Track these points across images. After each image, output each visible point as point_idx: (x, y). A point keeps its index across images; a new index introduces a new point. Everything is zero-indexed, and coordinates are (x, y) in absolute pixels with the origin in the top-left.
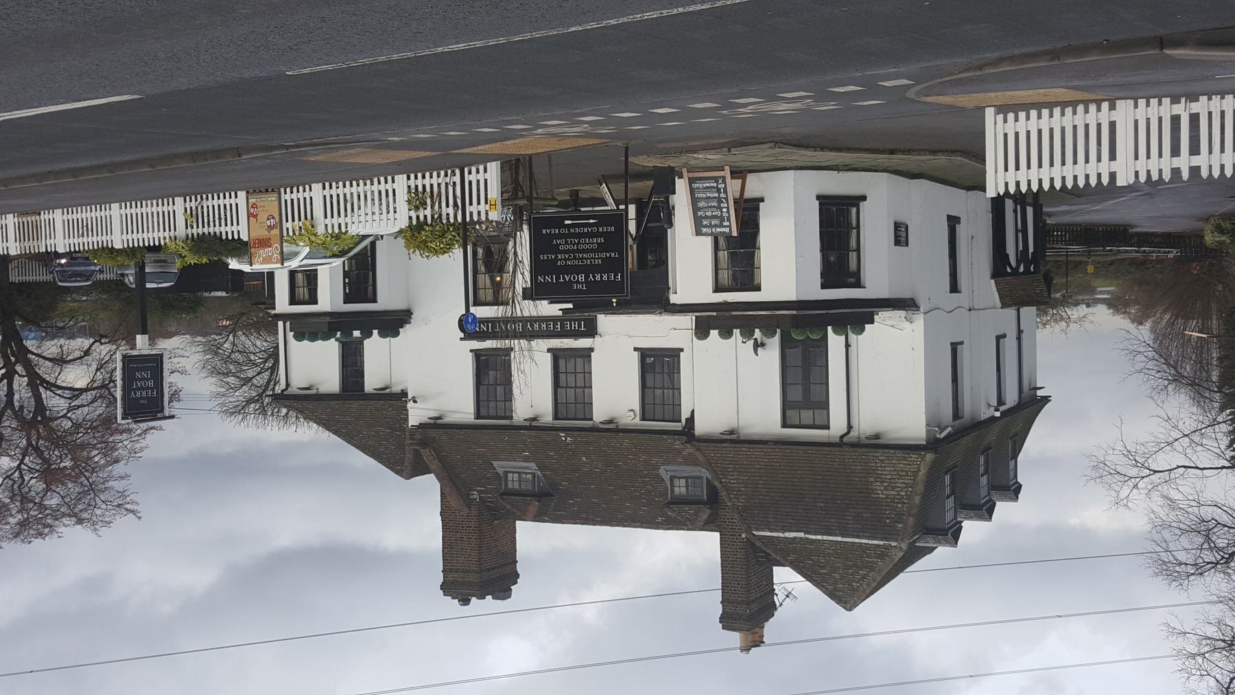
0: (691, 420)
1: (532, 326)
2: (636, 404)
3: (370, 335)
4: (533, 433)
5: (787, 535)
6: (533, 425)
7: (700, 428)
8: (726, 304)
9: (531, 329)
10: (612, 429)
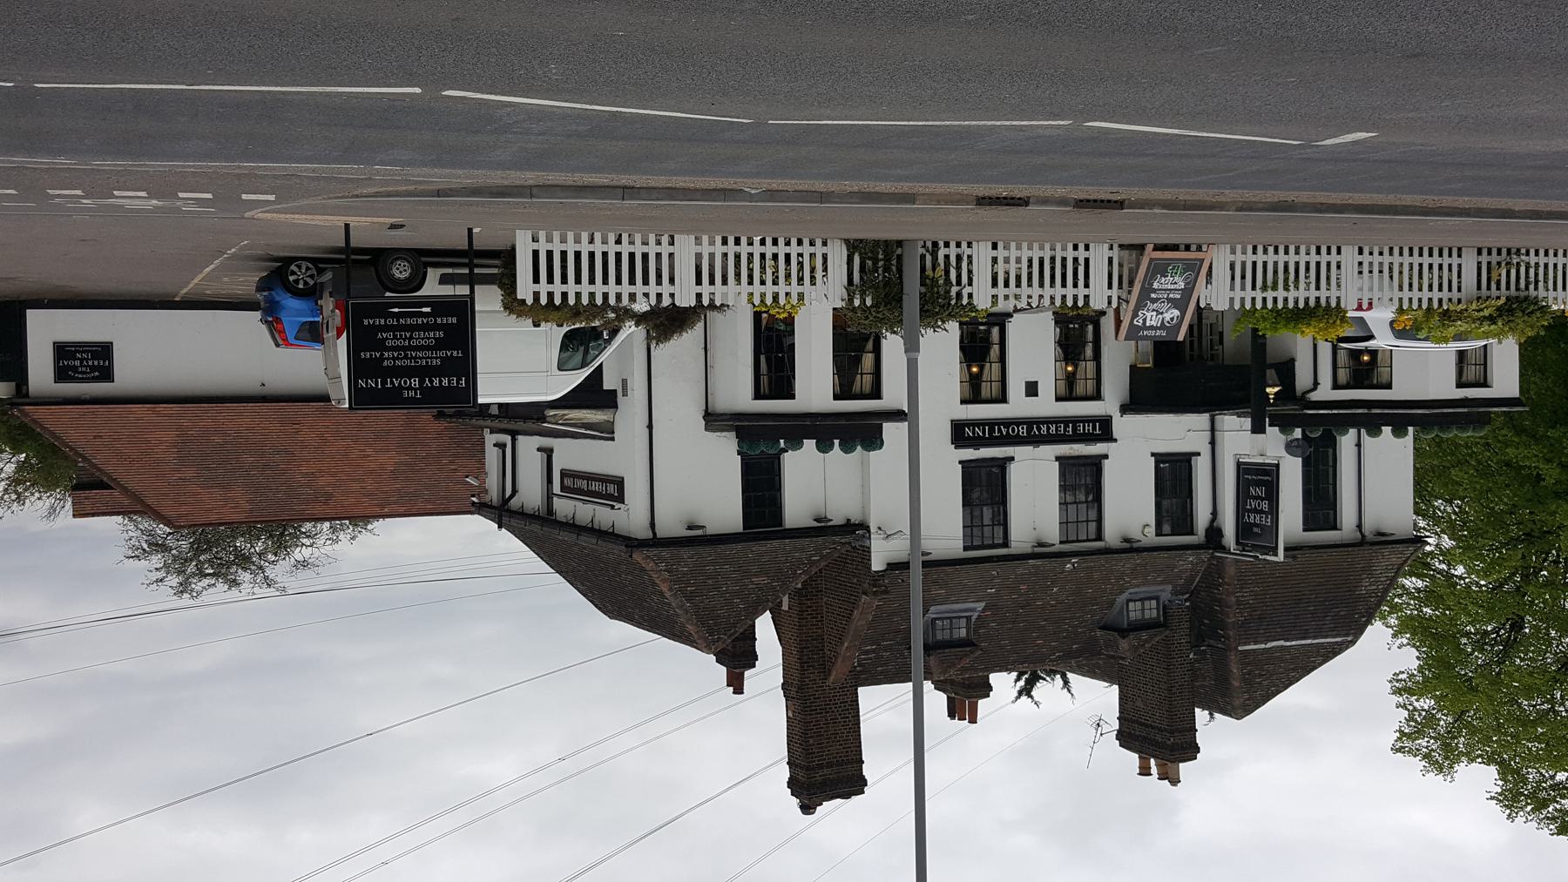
1: (1039, 429)
2: (1150, 516)
3: (798, 445)
6: (1040, 553)
8: (1466, 399)
9: (1034, 432)
10: (1130, 547)
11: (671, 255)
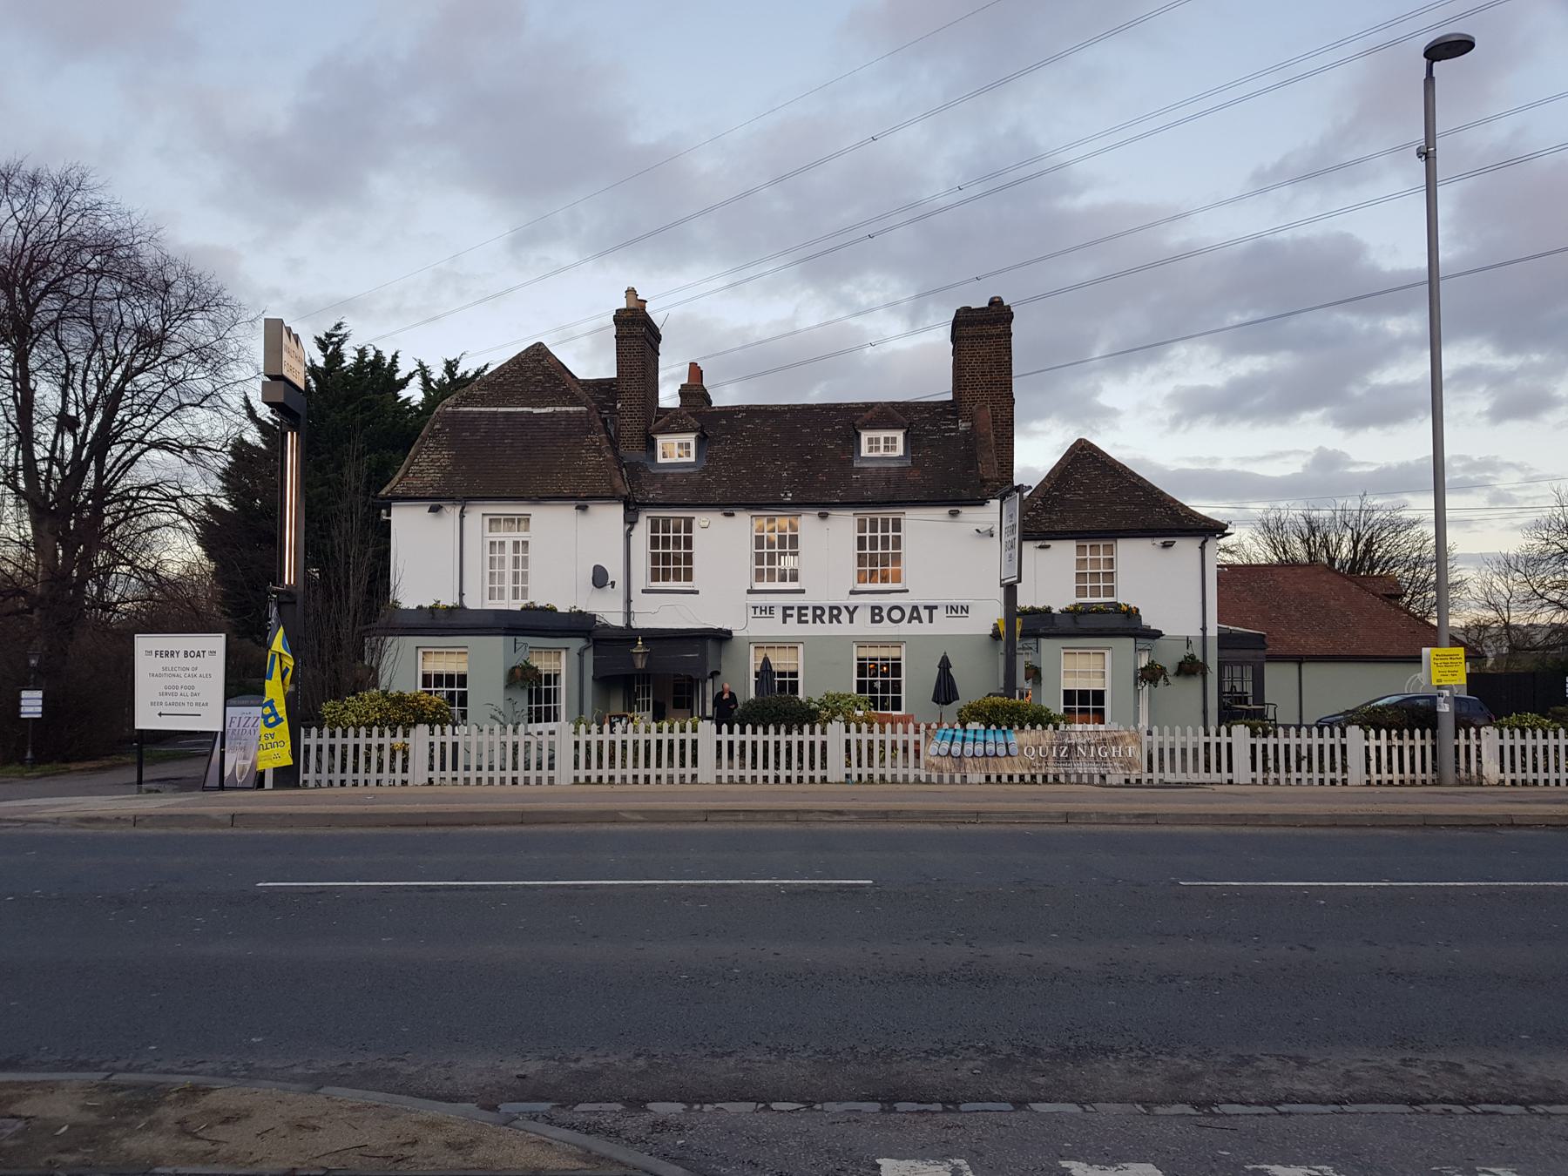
0: (630, 521)
4: (827, 500)
5: (550, 410)
6: (824, 505)
7: (617, 512)
10: (728, 506)
11: (431, 768)
